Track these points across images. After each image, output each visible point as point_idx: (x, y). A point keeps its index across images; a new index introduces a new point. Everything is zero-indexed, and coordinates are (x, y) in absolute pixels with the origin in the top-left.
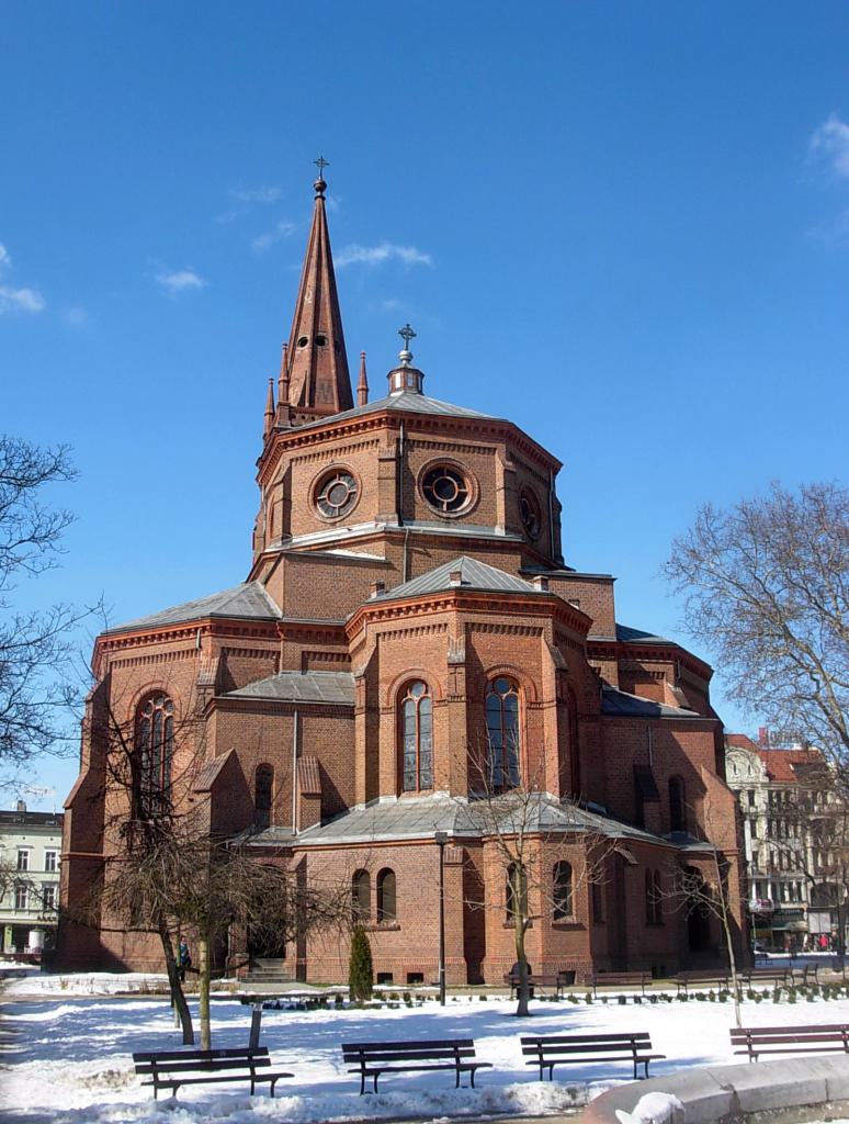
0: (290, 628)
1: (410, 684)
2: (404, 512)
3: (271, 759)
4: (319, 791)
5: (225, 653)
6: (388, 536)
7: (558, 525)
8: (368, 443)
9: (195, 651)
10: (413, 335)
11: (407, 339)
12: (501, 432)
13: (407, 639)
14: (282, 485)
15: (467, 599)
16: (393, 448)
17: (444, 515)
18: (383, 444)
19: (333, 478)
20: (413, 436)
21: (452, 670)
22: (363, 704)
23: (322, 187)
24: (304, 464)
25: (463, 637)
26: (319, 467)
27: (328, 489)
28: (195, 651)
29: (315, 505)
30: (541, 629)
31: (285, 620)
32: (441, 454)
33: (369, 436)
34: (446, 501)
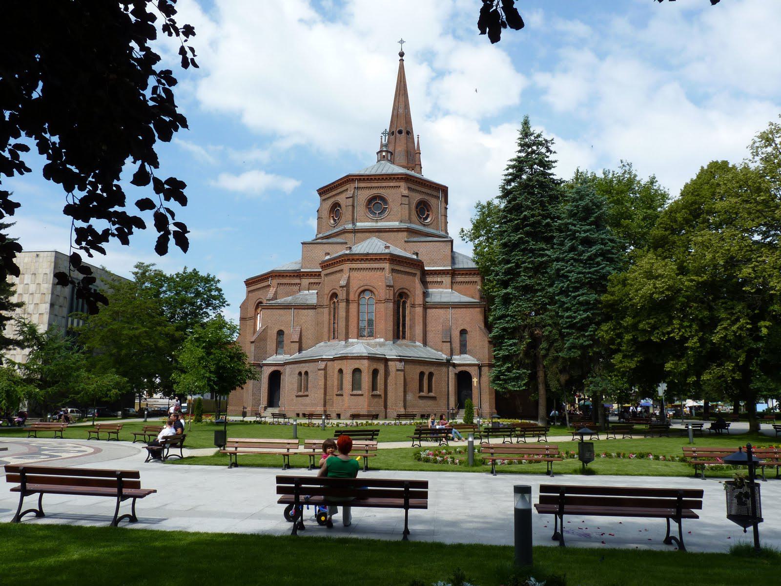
3: (282, 328)
4: (298, 340)
13: (332, 277)
16: (352, 192)
20: (362, 185)
21: (341, 289)
23: (402, 54)
24: (326, 202)
25: (348, 275)
26: (330, 202)
28: (269, 286)
29: (330, 219)
30: (384, 268)
31: (302, 270)
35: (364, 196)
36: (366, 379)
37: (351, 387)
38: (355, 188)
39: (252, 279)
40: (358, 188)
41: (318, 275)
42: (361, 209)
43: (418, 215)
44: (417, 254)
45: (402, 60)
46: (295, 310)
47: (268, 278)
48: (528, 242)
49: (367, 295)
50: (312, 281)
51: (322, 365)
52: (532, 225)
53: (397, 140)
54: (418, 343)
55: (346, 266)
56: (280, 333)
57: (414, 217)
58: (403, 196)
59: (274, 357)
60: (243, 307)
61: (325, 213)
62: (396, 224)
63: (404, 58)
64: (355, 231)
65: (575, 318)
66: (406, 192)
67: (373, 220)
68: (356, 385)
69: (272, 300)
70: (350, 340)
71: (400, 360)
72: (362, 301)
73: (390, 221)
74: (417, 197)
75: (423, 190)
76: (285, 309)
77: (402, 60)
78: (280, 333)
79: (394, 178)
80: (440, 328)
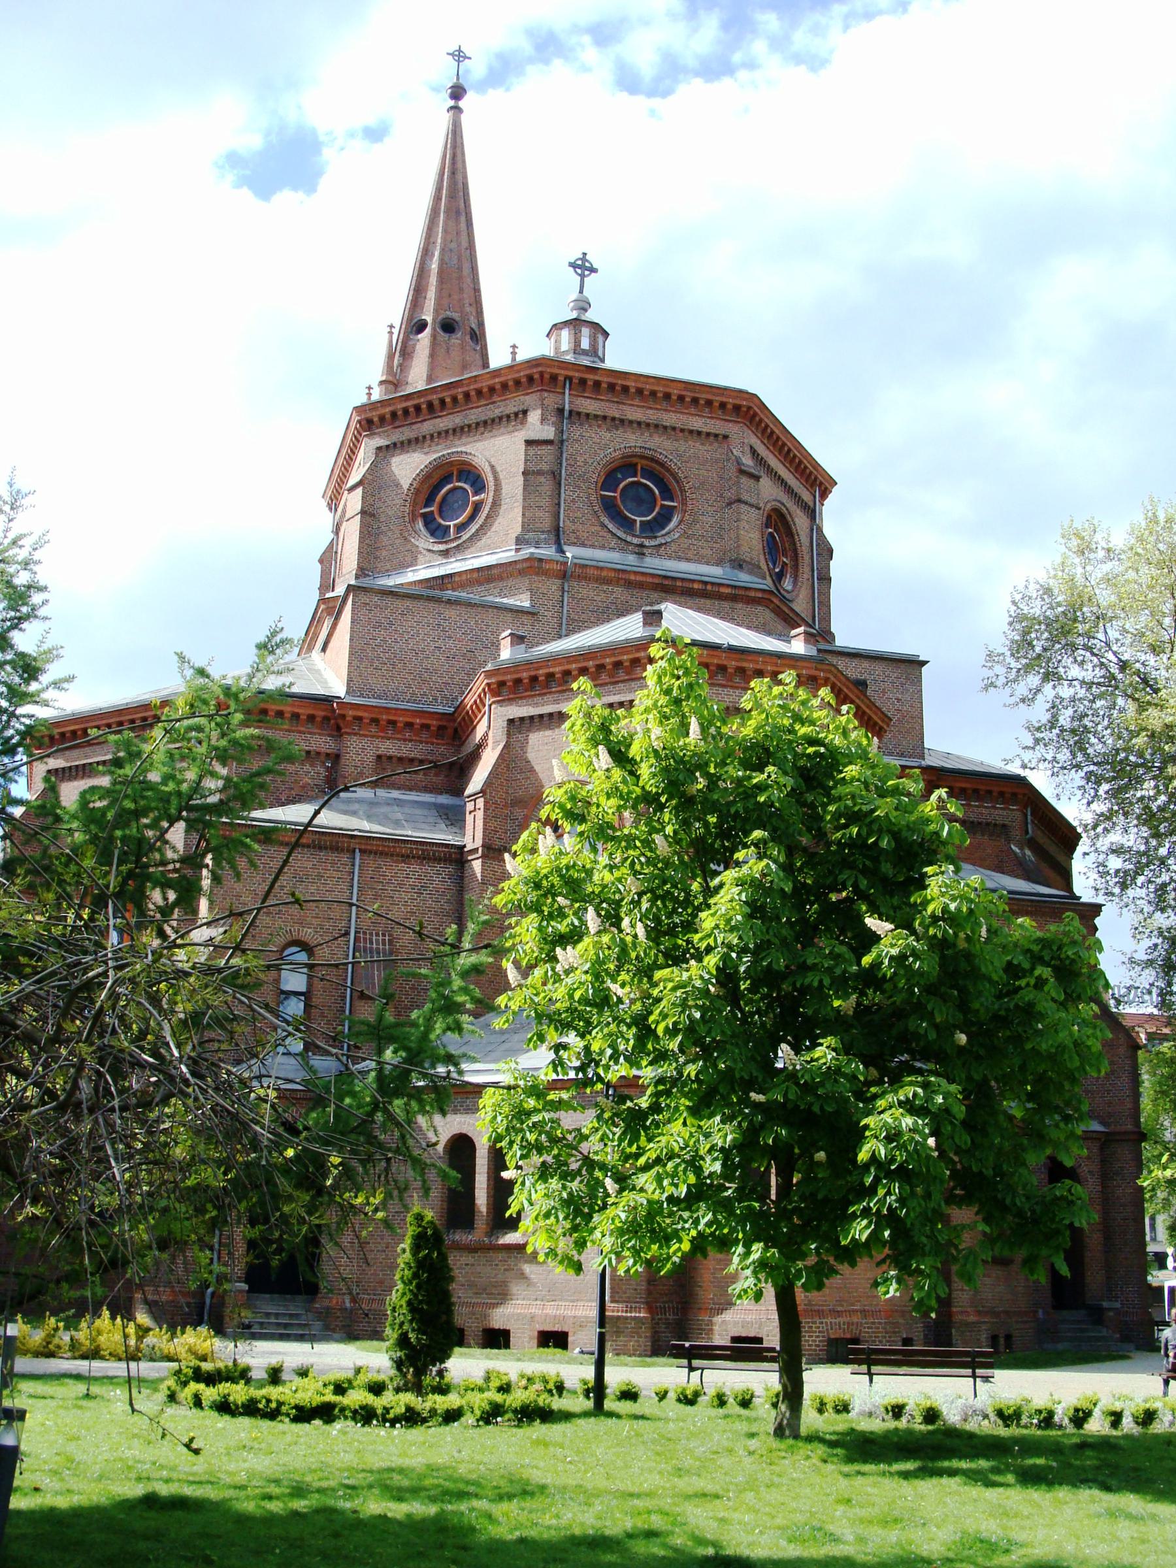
0: (360, 714)
6: (533, 568)
7: (826, 579)
8: (508, 416)
10: (593, 270)
11: (582, 276)
12: (737, 408)
14: (360, 490)
17: (636, 541)
18: (534, 417)
19: (446, 479)
20: (589, 405)
22: (479, 843)
23: (457, 93)
27: (439, 498)
29: (413, 520)
32: (633, 441)
33: (510, 405)
34: (638, 519)
35: (596, 447)
38: (561, 411)
40: (576, 416)
46: (370, 860)
50: (389, 747)
53: (441, 351)
58: (742, 472)
63: (461, 104)
66: (748, 461)
73: (688, 560)
74: (768, 491)
75: (783, 472)
76: (320, 848)
77: (456, 109)
79: (709, 403)
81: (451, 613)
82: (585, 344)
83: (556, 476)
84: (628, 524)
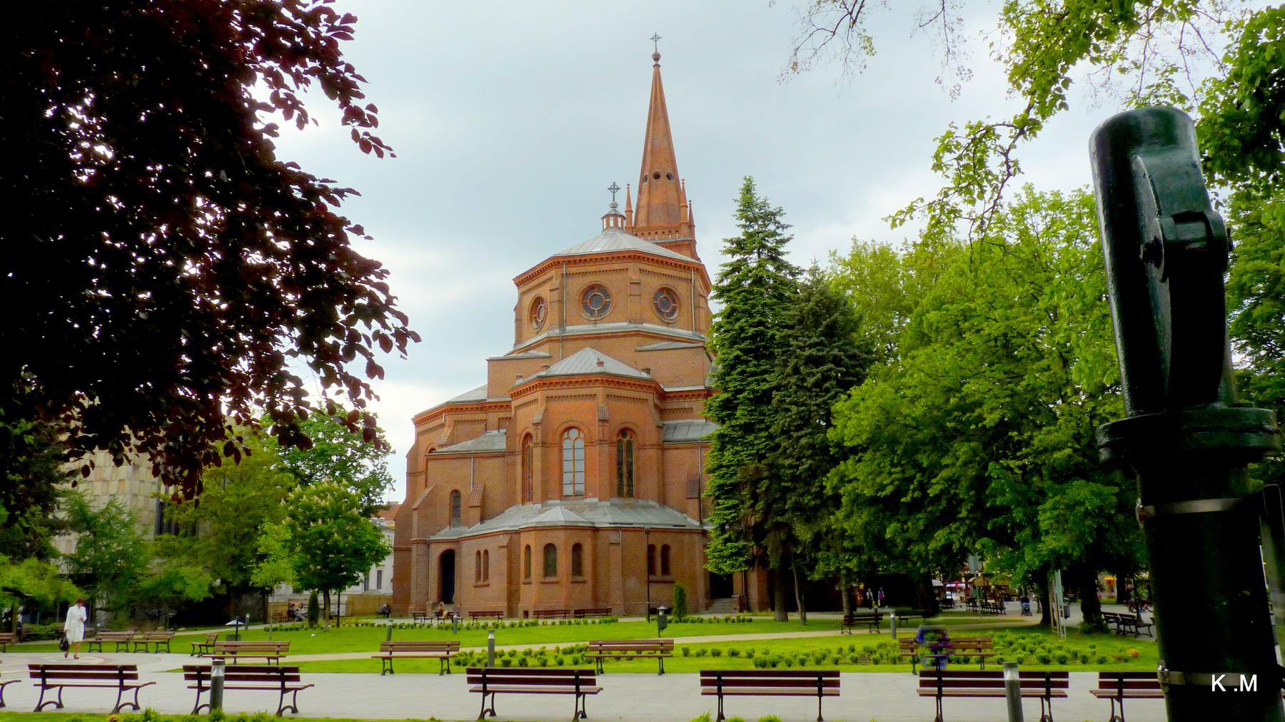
1: (528, 436)
2: (562, 324)
3: (457, 487)
5: (457, 422)
6: (550, 340)
9: (443, 425)
15: (546, 382)
20: (573, 270)
28: (443, 425)
36: (564, 561)
37: (541, 572)
39: (422, 414)
41: (506, 406)
42: (573, 307)
43: (658, 310)
44: (648, 371)
45: (657, 66)
47: (441, 413)
48: (746, 362)
49: (574, 433)
51: (504, 540)
52: (753, 337)
54: (651, 503)
55: (538, 395)
56: (456, 494)
57: (650, 313)
59: (447, 529)
60: (412, 456)
61: (526, 314)
62: (622, 325)
64: (563, 339)
65: (797, 467)
66: (635, 278)
67: (589, 322)
68: (550, 568)
69: (446, 445)
70: (550, 502)
71: (616, 529)
72: (567, 444)
77: (657, 66)
78: (456, 494)
80: (684, 479)
81: (521, 362)
82: (612, 224)
83: (561, 301)
84: (592, 313)
